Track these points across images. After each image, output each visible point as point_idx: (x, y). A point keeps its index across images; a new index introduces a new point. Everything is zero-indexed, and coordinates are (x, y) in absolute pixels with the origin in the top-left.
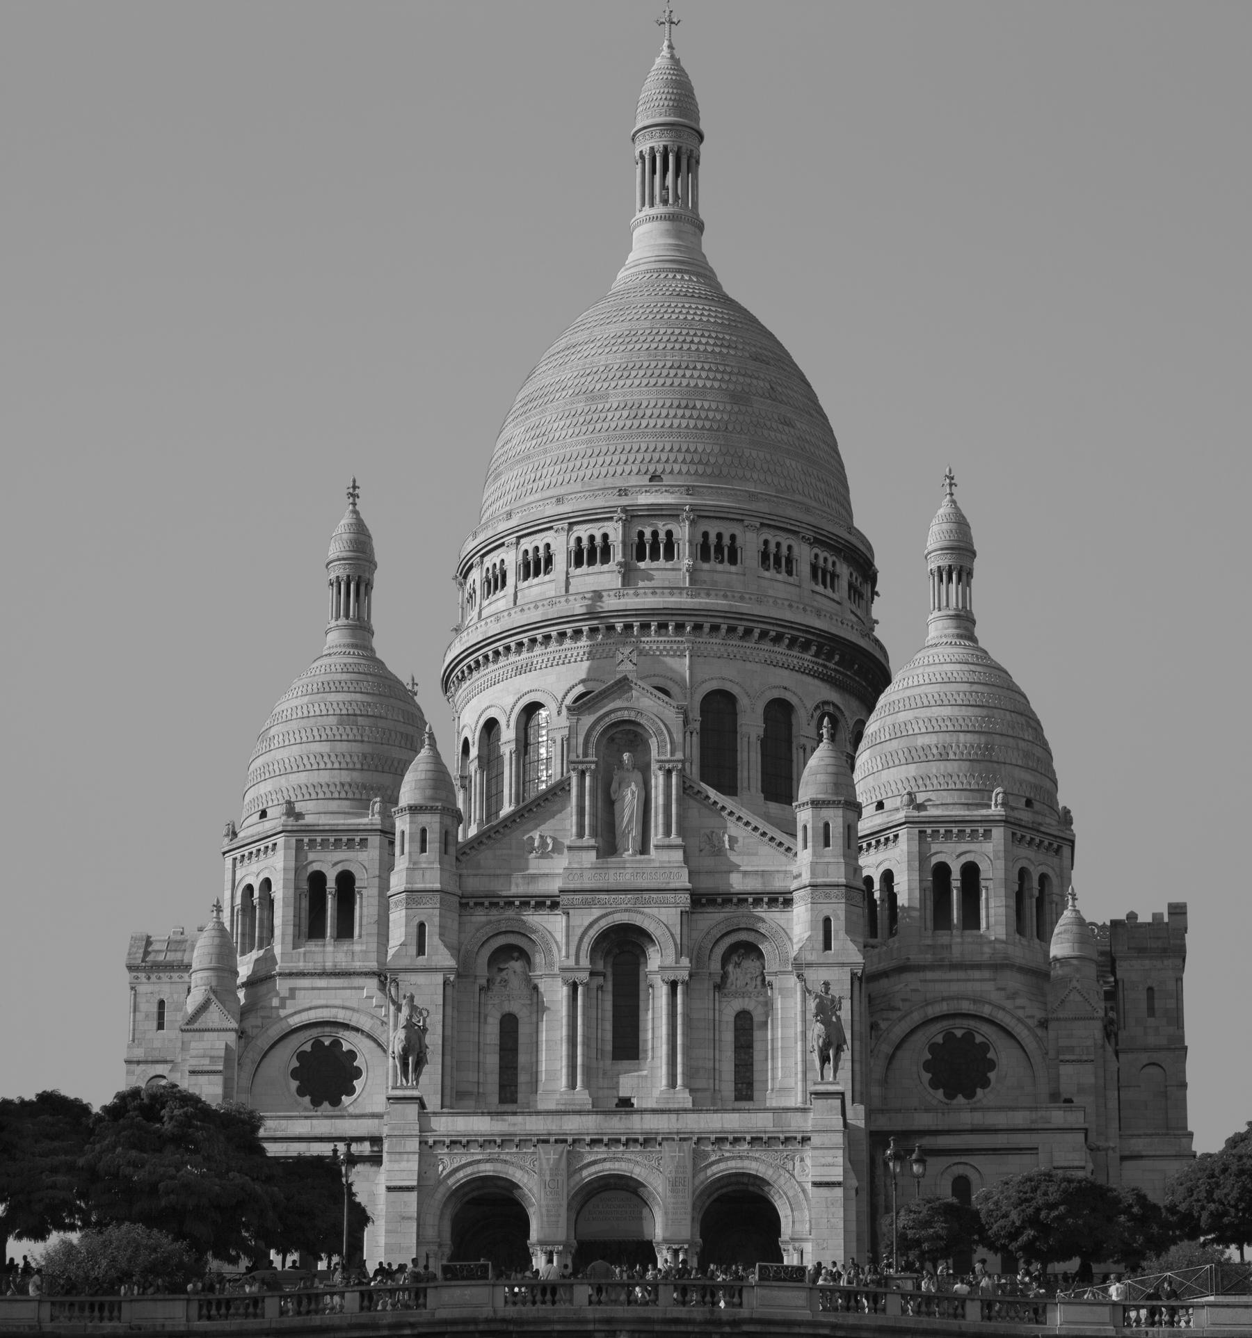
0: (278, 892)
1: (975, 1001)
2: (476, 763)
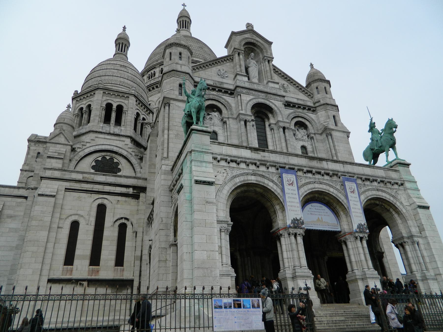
0: (93, 107)
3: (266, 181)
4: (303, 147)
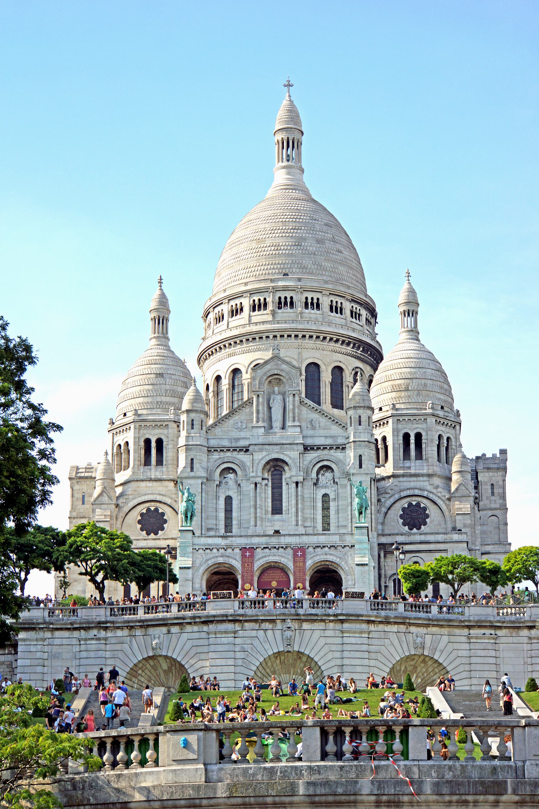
0: (131, 447)
1: (421, 489)
2: (212, 393)
3: (231, 560)
4: (325, 496)
